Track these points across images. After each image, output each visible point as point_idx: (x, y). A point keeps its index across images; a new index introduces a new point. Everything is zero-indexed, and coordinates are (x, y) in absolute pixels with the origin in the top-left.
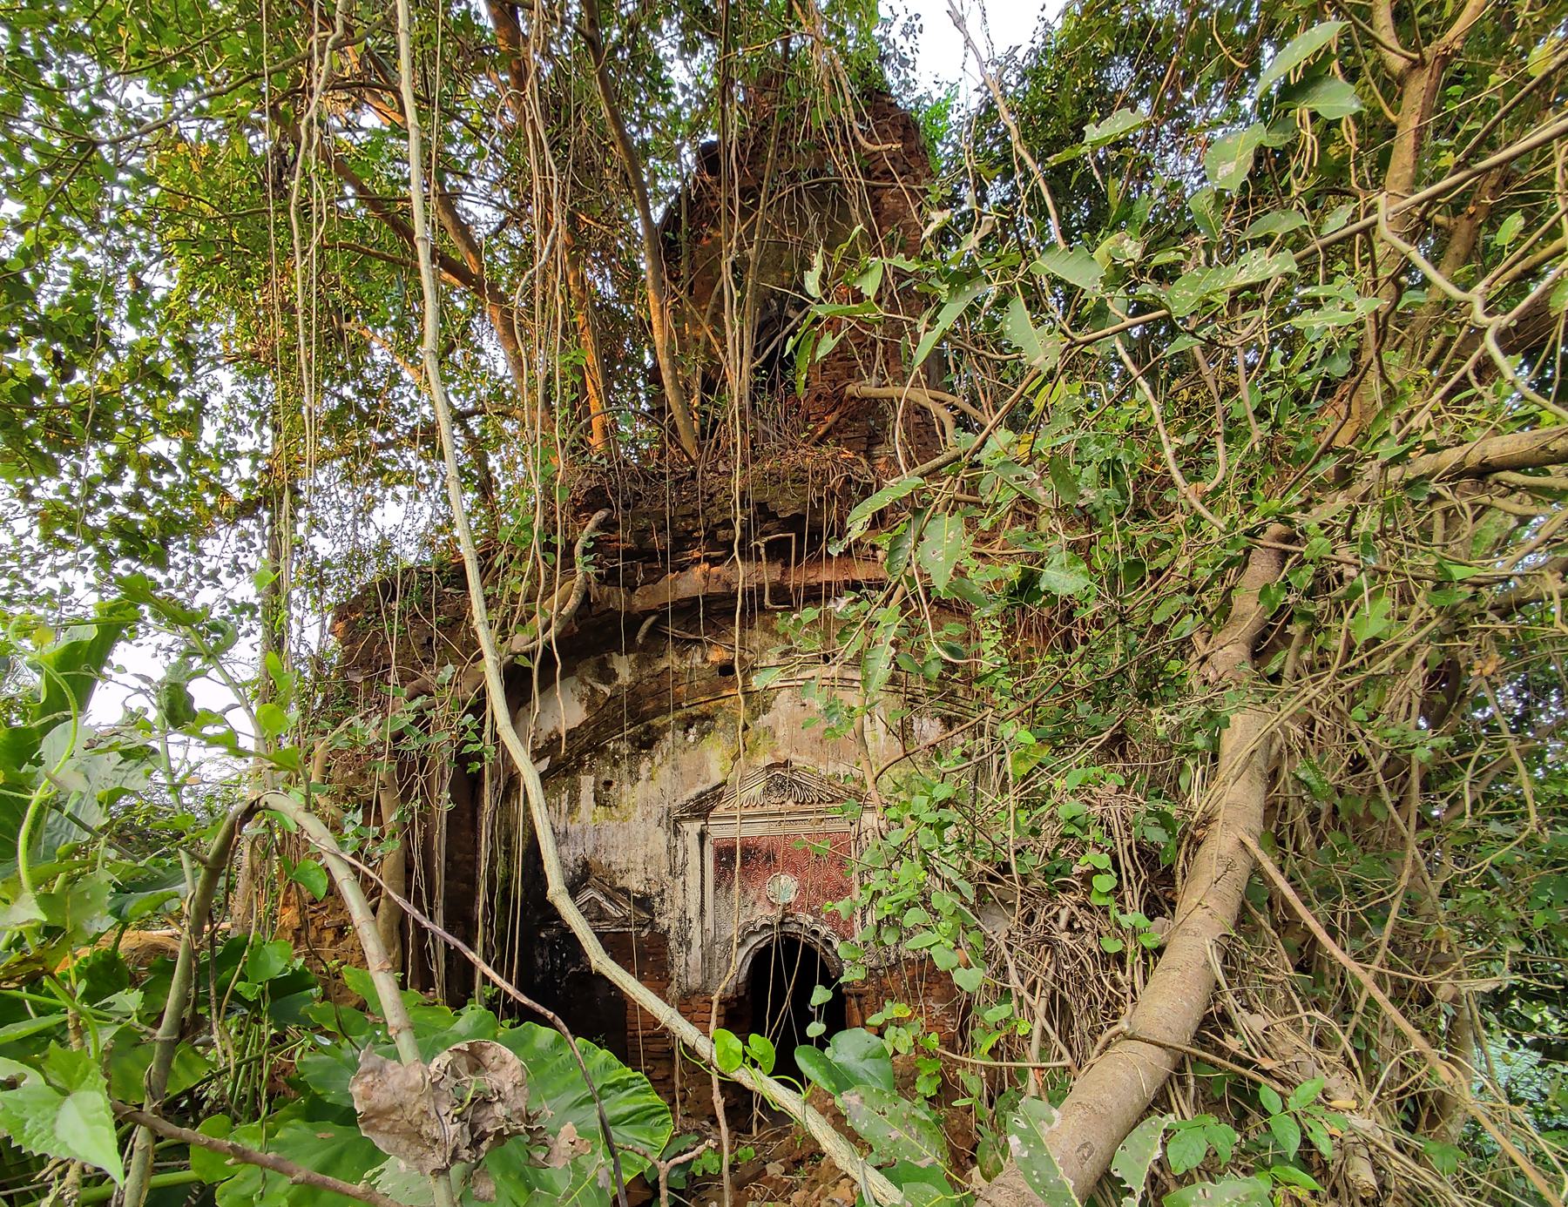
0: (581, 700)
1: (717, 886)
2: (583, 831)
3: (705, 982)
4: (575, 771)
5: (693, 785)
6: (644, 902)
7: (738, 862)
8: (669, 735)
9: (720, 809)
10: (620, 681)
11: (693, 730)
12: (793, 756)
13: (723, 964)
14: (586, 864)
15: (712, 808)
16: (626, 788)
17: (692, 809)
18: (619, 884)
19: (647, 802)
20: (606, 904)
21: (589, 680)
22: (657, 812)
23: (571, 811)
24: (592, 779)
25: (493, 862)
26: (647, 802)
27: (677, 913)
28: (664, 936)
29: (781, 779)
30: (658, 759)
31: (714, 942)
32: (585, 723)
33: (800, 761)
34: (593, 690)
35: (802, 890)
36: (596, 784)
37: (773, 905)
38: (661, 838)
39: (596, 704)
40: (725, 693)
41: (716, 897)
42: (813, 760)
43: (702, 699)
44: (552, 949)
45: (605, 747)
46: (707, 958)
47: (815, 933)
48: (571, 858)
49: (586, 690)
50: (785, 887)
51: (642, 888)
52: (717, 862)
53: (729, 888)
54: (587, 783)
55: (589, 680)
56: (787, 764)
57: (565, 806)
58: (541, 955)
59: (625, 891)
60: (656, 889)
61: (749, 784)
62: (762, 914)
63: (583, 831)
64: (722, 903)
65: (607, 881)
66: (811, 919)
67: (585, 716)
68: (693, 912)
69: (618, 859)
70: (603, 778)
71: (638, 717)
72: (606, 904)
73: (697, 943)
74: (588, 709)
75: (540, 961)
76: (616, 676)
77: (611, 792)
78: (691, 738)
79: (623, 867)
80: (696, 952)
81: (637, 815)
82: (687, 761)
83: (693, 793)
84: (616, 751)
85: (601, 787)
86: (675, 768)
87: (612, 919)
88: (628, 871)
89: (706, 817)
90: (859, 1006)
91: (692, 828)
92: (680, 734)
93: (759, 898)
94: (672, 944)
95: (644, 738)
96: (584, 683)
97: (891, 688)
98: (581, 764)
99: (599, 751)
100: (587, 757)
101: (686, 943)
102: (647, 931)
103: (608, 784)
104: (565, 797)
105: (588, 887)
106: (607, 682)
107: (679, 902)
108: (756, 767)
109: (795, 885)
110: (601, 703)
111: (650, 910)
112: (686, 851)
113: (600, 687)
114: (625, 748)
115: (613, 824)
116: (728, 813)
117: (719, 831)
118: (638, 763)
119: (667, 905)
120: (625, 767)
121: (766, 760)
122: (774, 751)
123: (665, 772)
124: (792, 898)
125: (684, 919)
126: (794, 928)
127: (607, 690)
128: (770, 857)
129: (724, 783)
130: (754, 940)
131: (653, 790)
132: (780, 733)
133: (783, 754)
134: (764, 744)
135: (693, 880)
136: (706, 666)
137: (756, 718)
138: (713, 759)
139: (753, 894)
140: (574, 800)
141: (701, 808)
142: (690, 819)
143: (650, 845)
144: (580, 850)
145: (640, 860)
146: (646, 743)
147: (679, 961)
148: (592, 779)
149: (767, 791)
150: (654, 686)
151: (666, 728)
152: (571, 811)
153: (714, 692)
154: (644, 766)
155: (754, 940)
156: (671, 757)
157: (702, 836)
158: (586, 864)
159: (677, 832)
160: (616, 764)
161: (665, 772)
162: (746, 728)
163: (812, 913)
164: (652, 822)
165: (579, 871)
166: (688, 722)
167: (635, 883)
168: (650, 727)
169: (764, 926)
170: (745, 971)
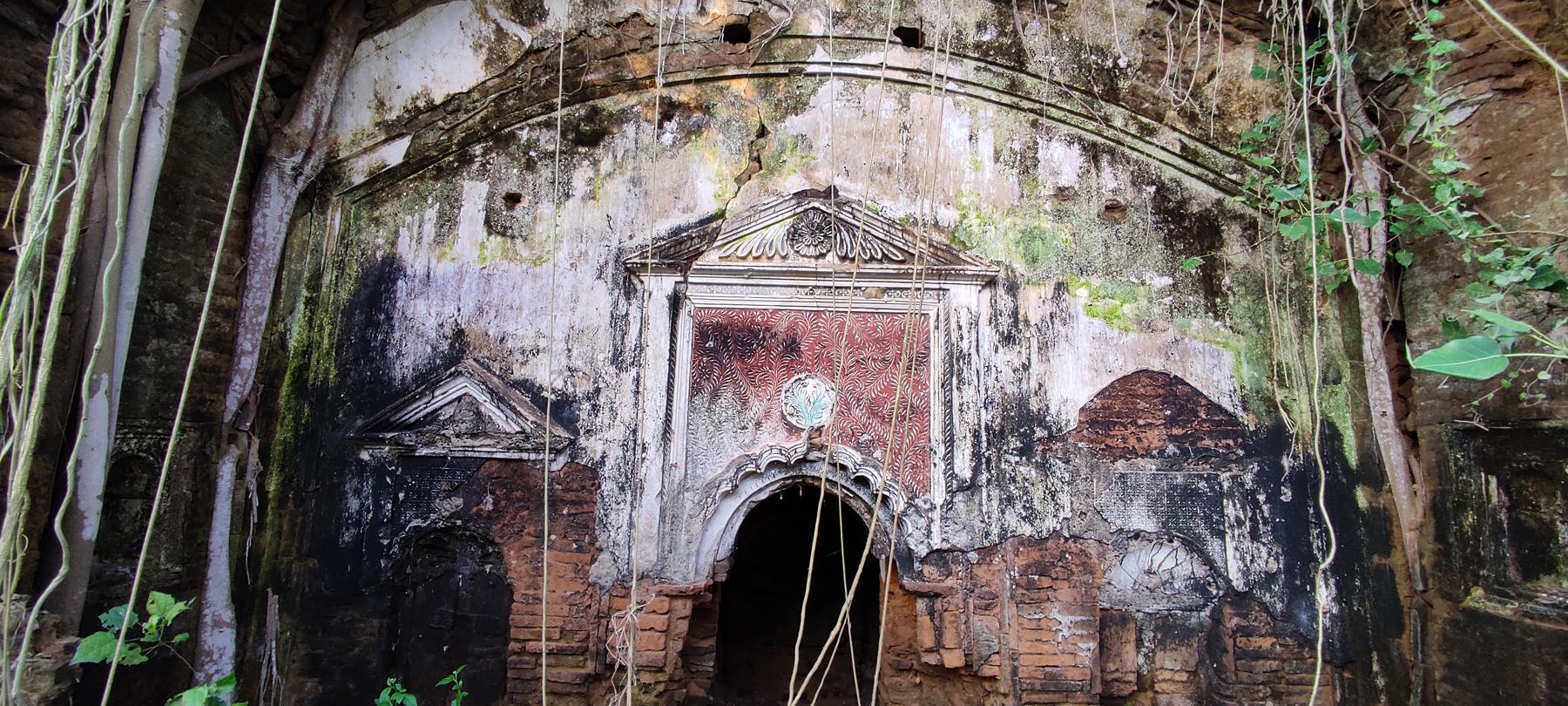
0: (477, 47)
1: (695, 389)
2: (460, 275)
3: (663, 558)
4: (456, 172)
5: (665, 213)
6: (563, 409)
7: (733, 351)
8: (630, 129)
9: (711, 258)
10: (549, 24)
11: (671, 126)
12: (839, 182)
13: (697, 526)
14: (459, 334)
15: (698, 254)
16: (546, 208)
17: (660, 252)
18: (519, 373)
19: (580, 236)
20: (489, 408)
21: (494, 13)
22: (598, 253)
23: (439, 240)
24: (483, 188)
25: (277, 314)
26: (580, 236)
27: (618, 433)
28: (592, 473)
29: (820, 217)
30: (606, 165)
31: (683, 488)
32: (481, 88)
33: (851, 189)
34: (499, 29)
35: (843, 408)
36: (490, 197)
37: (793, 430)
38: (599, 300)
39: (503, 57)
40: (731, 71)
41: (692, 409)
42: (873, 191)
43: (691, 76)
44: (379, 486)
45: (513, 136)
46: (669, 515)
47: (862, 482)
48: (432, 322)
49: (488, 31)
50: (813, 399)
51: (559, 384)
52: (699, 347)
53: (715, 395)
54: (474, 193)
55: (494, 13)
56: (830, 193)
57: (430, 229)
58: (358, 492)
59: (527, 386)
60: (584, 387)
61: (766, 218)
62: (772, 443)
63: (460, 275)
64: (702, 419)
65: (496, 367)
66: (858, 457)
67: (481, 75)
68: (650, 431)
69: (521, 331)
70: (504, 188)
71: (579, 93)
72: (489, 408)
73: (653, 485)
74: (488, 62)
75: (354, 504)
76: (543, 15)
77: (519, 211)
78: (667, 138)
79: (528, 344)
80: (650, 504)
81: (562, 257)
82: (661, 174)
83: (663, 227)
84: (532, 144)
85: (499, 203)
86: (635, 182)
87: (499, 434)
88: (537, 351)
89: (685, 269)
90: (931, 613)
91: (660, 286)
92: (649, 129)
93: (767, 414)
94: (608, 487)
95: (585, 128)
96: (485, 17)
97: (1006, 99)
98: (466, 160)
99: (502, 140)
100: (478, 149)
101: (631, 485)
102: (562, 459)
103: (513, 199)
104: (431, 214)
105: (460, 374)
106: (527, 23)
107: (626, 413)
108: (780, 195)
109: (829, 399)
110: (513, 57)
111: (570, 423)
112: (644, 322)
113: (513, 29)
114: (549, 141)
115: (516, 269)
116: (725, 265)
117: (712, 296)
118: (568, 168)
119: (604, 417)
120: (545, 173)
121: (793, 182)
122: (808, 171)
123: (617, 188)
124: (826, 419)
125: (633, 442)
126: (822, 471)
127: (526, 37)
128: (792, 347)
129: (721, 215)
130: (750, 487)
131: (593, 216)
132: (821, 142)
133: (823, 178)
134: (792, 160)
135: (655, 377)
136: (703, 21)
137: (783, 117)
138: (705, 177)
139: (757, 408)
140: (448, 222)
141: (678, 252)
142: (657, 270)
143: (580, 309)
144: (450, 309)
145: (560, 335)
146: (589, 135)
147: (619, 518)
148: (483, 188)
149: (794, 236)
150: (610, 42)
151: (622, 117)
152: (439, 240)
153: (712, 77)
154: (581, 176)
155: (750, 487)
156: (630, 164)
157: (676, 302)
158: (459, 334)
159: (629, 292)
160: (530, 166)
161: (617, 188)
162: (763, 132)
163: (858, 447)
164: (587, 271)
165: (445, 346)
166: (669, 109)
167: (546, 374)
168: (595, 111)
169: (774, 464)
170: (730, 539)
